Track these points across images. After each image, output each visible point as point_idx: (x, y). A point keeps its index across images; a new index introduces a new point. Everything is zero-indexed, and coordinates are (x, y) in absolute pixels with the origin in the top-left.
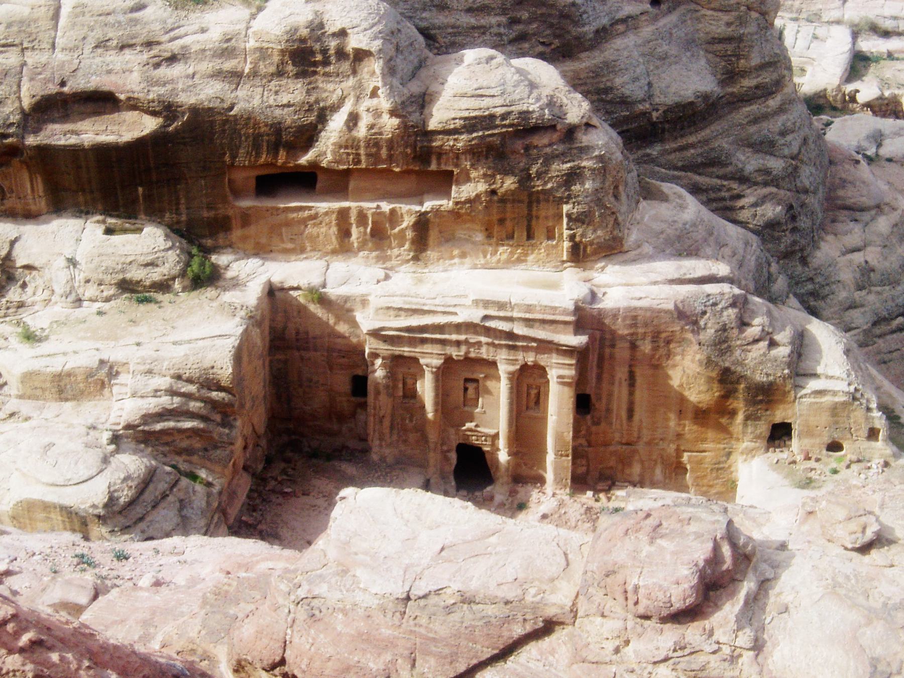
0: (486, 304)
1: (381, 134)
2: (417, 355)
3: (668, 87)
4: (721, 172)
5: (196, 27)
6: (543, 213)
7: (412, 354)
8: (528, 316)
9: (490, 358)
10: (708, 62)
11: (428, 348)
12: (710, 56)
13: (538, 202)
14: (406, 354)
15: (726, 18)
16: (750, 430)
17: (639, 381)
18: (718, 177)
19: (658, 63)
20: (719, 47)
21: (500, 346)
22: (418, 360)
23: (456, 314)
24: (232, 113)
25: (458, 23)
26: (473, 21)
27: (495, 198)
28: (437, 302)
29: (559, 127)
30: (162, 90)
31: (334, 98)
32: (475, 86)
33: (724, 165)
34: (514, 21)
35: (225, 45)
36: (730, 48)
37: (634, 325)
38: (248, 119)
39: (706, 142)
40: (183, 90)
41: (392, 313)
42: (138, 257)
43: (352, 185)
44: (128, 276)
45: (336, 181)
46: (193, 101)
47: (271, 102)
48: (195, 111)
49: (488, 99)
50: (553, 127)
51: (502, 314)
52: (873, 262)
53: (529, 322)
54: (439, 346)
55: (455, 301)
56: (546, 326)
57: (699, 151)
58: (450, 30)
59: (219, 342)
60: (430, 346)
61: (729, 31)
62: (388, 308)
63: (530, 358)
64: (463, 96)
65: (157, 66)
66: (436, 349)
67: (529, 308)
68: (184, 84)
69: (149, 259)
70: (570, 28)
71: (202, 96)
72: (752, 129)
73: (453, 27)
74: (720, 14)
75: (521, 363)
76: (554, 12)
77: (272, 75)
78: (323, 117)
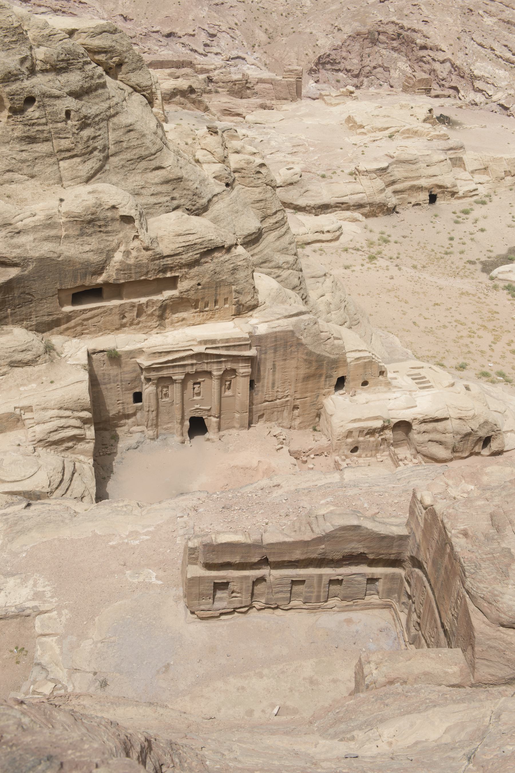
0: (205, 342)
1: (142, 260)
2: (171, 375)
3: (243, 226)
4: (271, 265)
5: (28, 213)
6: (222, 292)
7: (168, 375)
8: (227, 344)
9: (209, 370)
10: (255, 213)
11: (177, 370)
12: (254, 210)
13: (220, 287)
14: (165, 376)
15: (258, 190)
16: (328, 383)
17: (277, 368)
18: (269, 268)
19: (236, 215)
20: (258, 205)
21: (214, 362)
22: (171, 378)
23: (191, 350)
24: (60, 259)
25: (149, 202)
26: (155, 201)
27: (200, 287)
28: (179, 346)
29: (226, 246)
30: (18, 251)
31: (114, 244)
32: (184, 230)
33: (270, 261)
34: (173, 199)
35: (49, 222)
36: (262, 204)
37: (276, 341)
38: (69, 261)
39: (261, 251)
40: (31, 250)
41: (157, 355)
42: (17, 348)
43: (124, 292)
44: (14, 359)
45: (116, 290)
46: (37, 255)
47: (81, 251)
48: (41, 260)
49: (192, 236)
50: (223, 246)
51: (214, 346)
52: (330, 300)
53: (227, 348)
54: (182, 369)
55: (189, 343)
56: (236, 348)
57: (260, 256)
58: (145, 207)
59: (78, 385)
60: (177, 369)
61: (261, 197)
62: (154, 353)
63: (229, 366)
64: (179, 235)
65: (12, 237)
66: (180, 370)
67: (227, 340)
68: (30, 246)
69: (24, 347)
70: (198, 200)
71: (42, 252)
72: (278, 243)
73: (147, 205)
74: (255, 188)
75: (223, 370)
76: (190, 193)
77: (78, 235)
78: (109, 257)
